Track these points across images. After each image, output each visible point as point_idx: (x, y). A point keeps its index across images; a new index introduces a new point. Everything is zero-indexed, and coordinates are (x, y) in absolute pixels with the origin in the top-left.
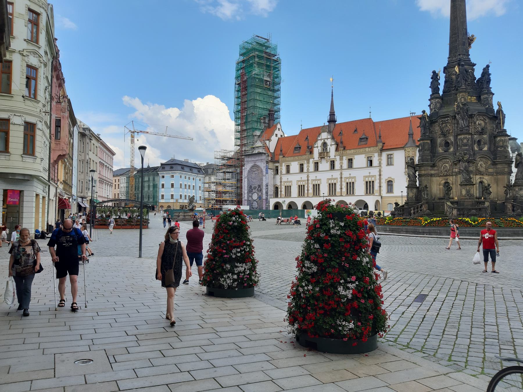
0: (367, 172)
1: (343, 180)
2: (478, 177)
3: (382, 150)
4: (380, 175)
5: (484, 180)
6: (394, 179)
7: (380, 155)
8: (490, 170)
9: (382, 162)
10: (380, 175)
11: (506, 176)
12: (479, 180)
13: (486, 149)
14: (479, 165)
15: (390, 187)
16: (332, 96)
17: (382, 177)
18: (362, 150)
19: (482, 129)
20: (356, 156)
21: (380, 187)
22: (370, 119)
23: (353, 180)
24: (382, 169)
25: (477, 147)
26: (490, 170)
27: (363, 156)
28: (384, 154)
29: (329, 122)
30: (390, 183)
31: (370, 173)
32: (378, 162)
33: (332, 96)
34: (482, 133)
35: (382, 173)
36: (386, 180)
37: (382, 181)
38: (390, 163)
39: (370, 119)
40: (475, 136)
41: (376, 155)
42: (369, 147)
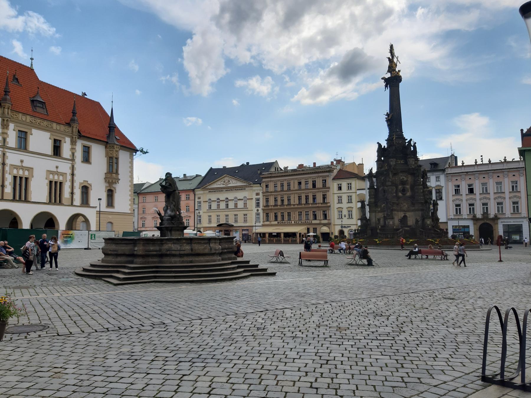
0: (52, 164)
1: (7, 168)
4: (73, 175)
7: (73, 143)
9: (76, 154)
10: (73, 175)
15: (85, 196)
17: (75, 178)
18: (45, 123)
20: (34, 131)
21: (72, 193)
23: (26, 173)
24: (75, 166)
27: (47, 135)
30: (85, 189)
31: (57, 167)
32: (70, 153)
35: (75, 172)
36: (81, 183)
37: (75, 184)
38: (87, 159)
41: (68, 140)
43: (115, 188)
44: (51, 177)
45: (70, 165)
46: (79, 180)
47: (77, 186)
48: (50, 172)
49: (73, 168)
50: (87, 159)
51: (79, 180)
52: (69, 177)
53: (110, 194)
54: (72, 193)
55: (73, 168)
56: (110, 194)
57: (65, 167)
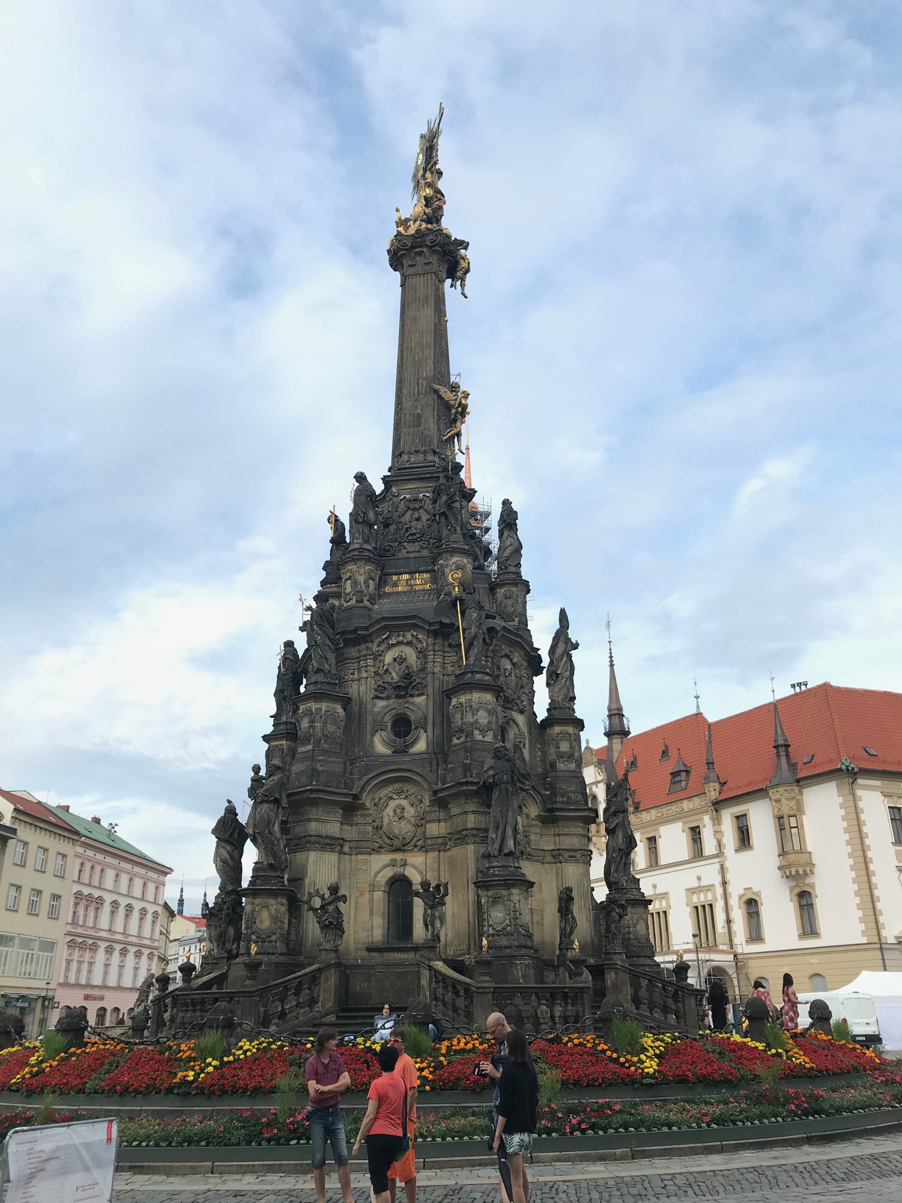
2: (380, 860)
3: (718, 805)
4: (724, 883)
5: (410, 872)
6: (758, 894)
7: (717, 821)
8: (434, 829)
10: (724, 883)
11: (471, 847)
12: (389, 873)
13: (421, 746)
14: (389, 811)
16: (612, 665)
17: (730, 889)
19: (408, 676)
21: (729, 921)
22: (698, 715)
24: (727, 865)
25: (386, 743)
26: (434, 829)
28: (727, 817)
29: (607, 734)
31: (699, 879)
32: (715, 843)
33: (612, 665)
34: (406, 686)
35: (728, 877)
38: (744, 839)
39: (698, 715)
40: (381, 703)
41: (707, 819)
42: (689, 798)
43: (812, 886)
44: (695, 898)
45: (718, 866)
46: (736, 891)
47: (734, 902)
48: (691, 891)
49: (723, 870)
50: (744, 839)
51: (736, 891)
52: (719, 890)
53: (805, 901)
54: (729, 921)
55: (723, 870)
56: (805, 901)
57: (709, 873)
